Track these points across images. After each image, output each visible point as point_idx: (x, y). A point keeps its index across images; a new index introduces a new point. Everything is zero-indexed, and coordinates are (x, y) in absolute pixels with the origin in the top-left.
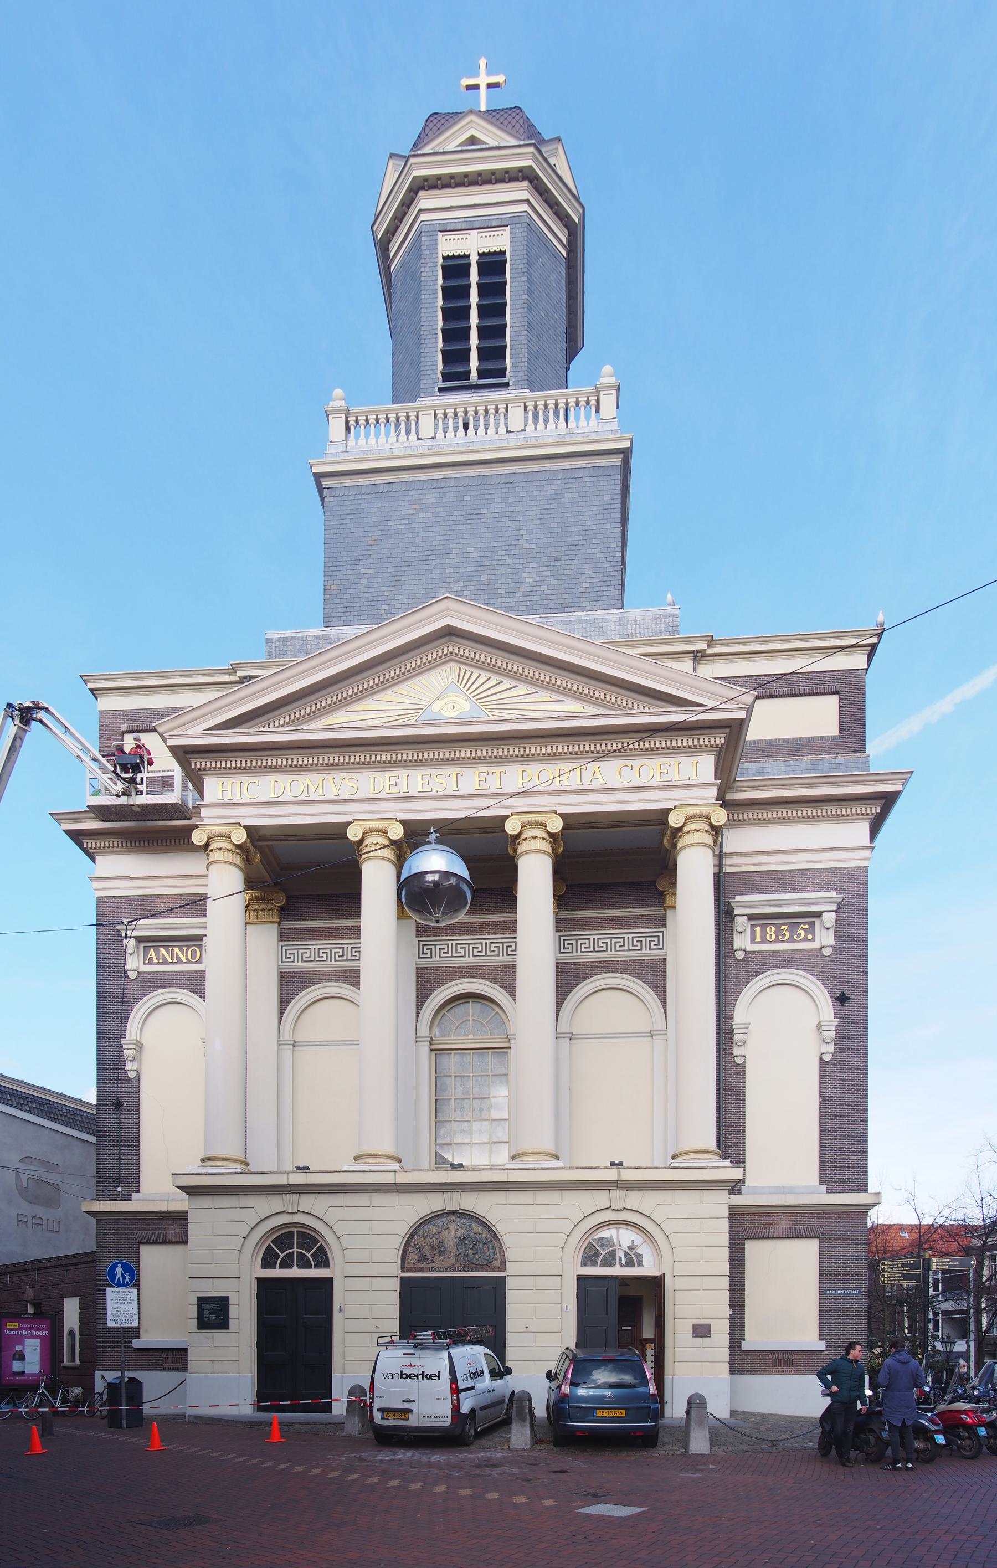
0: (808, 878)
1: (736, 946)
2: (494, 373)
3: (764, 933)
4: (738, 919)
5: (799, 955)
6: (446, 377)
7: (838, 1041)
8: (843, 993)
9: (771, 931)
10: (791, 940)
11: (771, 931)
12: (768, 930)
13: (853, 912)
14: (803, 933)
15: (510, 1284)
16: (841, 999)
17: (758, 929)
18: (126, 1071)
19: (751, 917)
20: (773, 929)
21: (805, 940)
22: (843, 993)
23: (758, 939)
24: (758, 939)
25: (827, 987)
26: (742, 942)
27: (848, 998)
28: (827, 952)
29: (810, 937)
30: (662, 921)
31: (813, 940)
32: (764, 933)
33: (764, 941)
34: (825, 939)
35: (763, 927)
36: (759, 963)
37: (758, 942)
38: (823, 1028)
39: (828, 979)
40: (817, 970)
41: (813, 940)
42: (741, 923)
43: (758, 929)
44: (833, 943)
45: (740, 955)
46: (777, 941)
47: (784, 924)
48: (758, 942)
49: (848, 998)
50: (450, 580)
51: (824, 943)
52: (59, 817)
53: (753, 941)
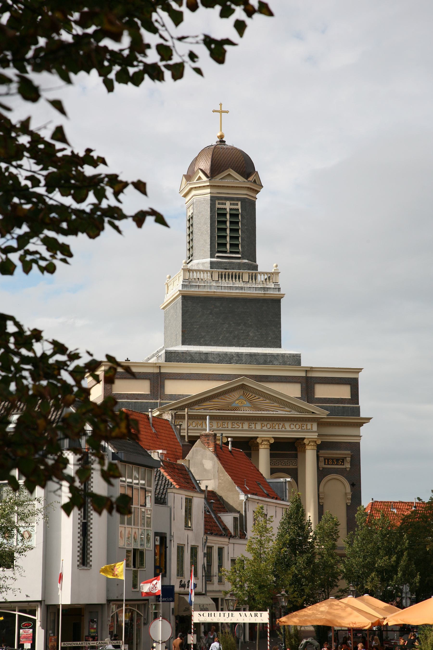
3: (328, 462)
7: (352, 499)
9: (330, 461)
10: (337, 464)
17: (326, 460)
21: (341, 465)
23: (326, 463)
24: (326, 463)
25: (348, 481)
27: (355, 485)
28: (348, 470)
30: (296, 456)
31: (344, 465)
32: (328, 462)
33: (328, 464)
34: (347, 466)
41: (344, 465)
43: (326, 460)
44: (350, 467)
49: (355, 485)
50: (225, 332)
51: (347, 467)
53: (325, 464)
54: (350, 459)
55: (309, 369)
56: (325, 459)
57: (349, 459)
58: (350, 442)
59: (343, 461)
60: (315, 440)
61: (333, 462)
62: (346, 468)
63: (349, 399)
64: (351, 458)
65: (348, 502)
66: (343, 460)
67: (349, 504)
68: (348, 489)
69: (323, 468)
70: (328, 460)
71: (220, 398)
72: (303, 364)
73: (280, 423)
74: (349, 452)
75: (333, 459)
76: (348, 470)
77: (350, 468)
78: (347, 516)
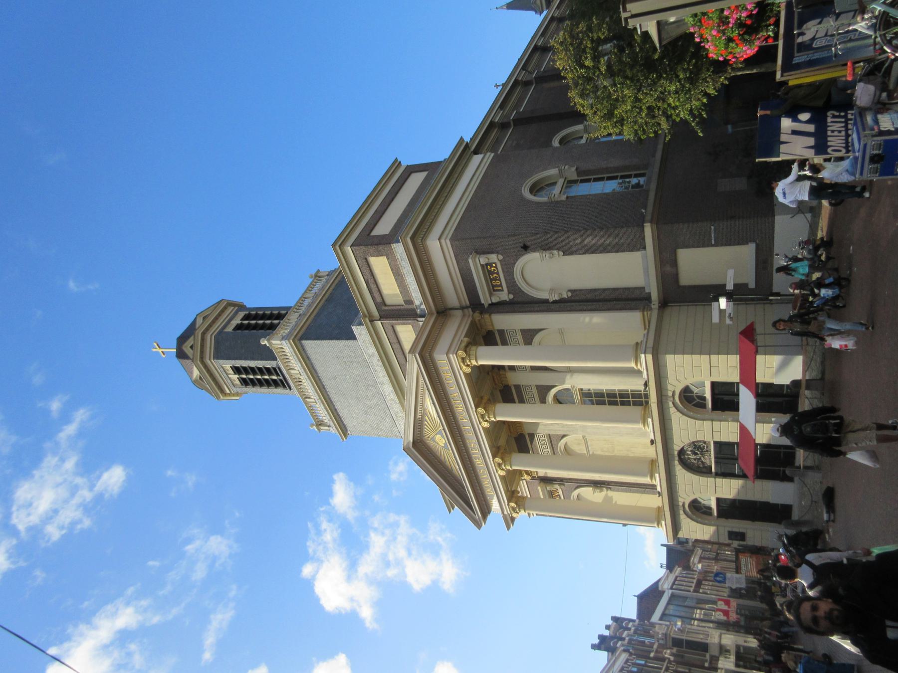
4: (494, 301)
6: (284, 386)
10: (497, 273)
15: (717, 439)
16: (526, 248)
19: (491, 295)
21: (496, 267)
26: (504, 295)
28: (501, 257)
33: (501, 285)
34: (494, 258)
35: (493, 286)
36: (513, 287)
45: (511, 296)
46: (500, 280)
55: (367, 320)
56: (494, 290)
57: (483, 260)
58: (455, 256)
59: (491, 265)
61: (495, 279)
62: (500, 261)
66: (487, 265)
67: (561, 253)
69: (509, 293)
70: (493, 286)
74: (470, 261)
75: (491, 280)
77: (498, 253)
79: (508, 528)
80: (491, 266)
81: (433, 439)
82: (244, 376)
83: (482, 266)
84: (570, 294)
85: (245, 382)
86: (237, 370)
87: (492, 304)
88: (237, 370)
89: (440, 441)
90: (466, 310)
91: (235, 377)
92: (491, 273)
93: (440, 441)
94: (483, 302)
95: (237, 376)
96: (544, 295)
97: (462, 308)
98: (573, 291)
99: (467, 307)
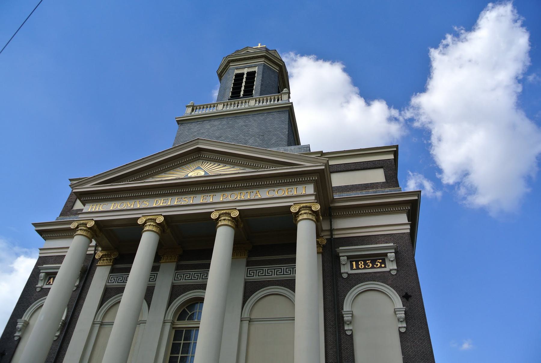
0: (378, 239)
1: (342, 271)
2: (249, 93)
3: (357, 265)
4: (341, 258)
5: (378, 275)
8: (406, 293)
9: (361, 264)
10: (373, 267)
11: (361, 264)
12: (360, 263)
13: (405, 253)
14: (379, 264)
16: (406, 297)
17: (354, 263)
18: (14, 337)
19: (349, 257)
20: (363, 263)
21: (381, 267)
22: (406, 293)
23: (354, 267)
24: (354, 267)
26: (346, 269)
27: (410, 296)
29: (383, 266)
31: (385, 267)
32: (357, 265)
33: (358, 268)
34: (391, 266)
37: (355, 269)
38: (397, 313)
39: (396, 286)
40: (390, 282)
41: (385, 267)
42: (343, 259)
43: (354, 263)
44: (395, 267)
46: (365, 268)
47: (369, 260)
48: (355, 269)
51: (391, 268)
52: (35, 225)
53: (352, 268)
54: (393, 254)
59: (384, 262)
60: (308, 205)
61: (365, 264)
63: (383, 182)
64: (396, 253)
65: (400, 326)
67: (403, 330)
68: (398, 303)
69: (349, 275)
71: (168, 173)
72: (312, 151)
73: (251, 191)
74: (392, 244)
76: (393, 273)
78: (403, 353)
79: (35, 225)
80: (381, 263)
81: (199, 168)
82: (245, 76)
83: (386, 255)
84: (349, 333)
85: (239, 77)
86: (251, 75)
87: (338, 257)
88: (251, 75)
89: (195, 172)
90: (328, 233)
91: (246, 71)
92: (373, 262)
93: (195, 172)
94: (340, 248)
95: (245, 73)
96: (346, 307)
97: (331, 230)
98: (351, 336)
99: (332, 235)
